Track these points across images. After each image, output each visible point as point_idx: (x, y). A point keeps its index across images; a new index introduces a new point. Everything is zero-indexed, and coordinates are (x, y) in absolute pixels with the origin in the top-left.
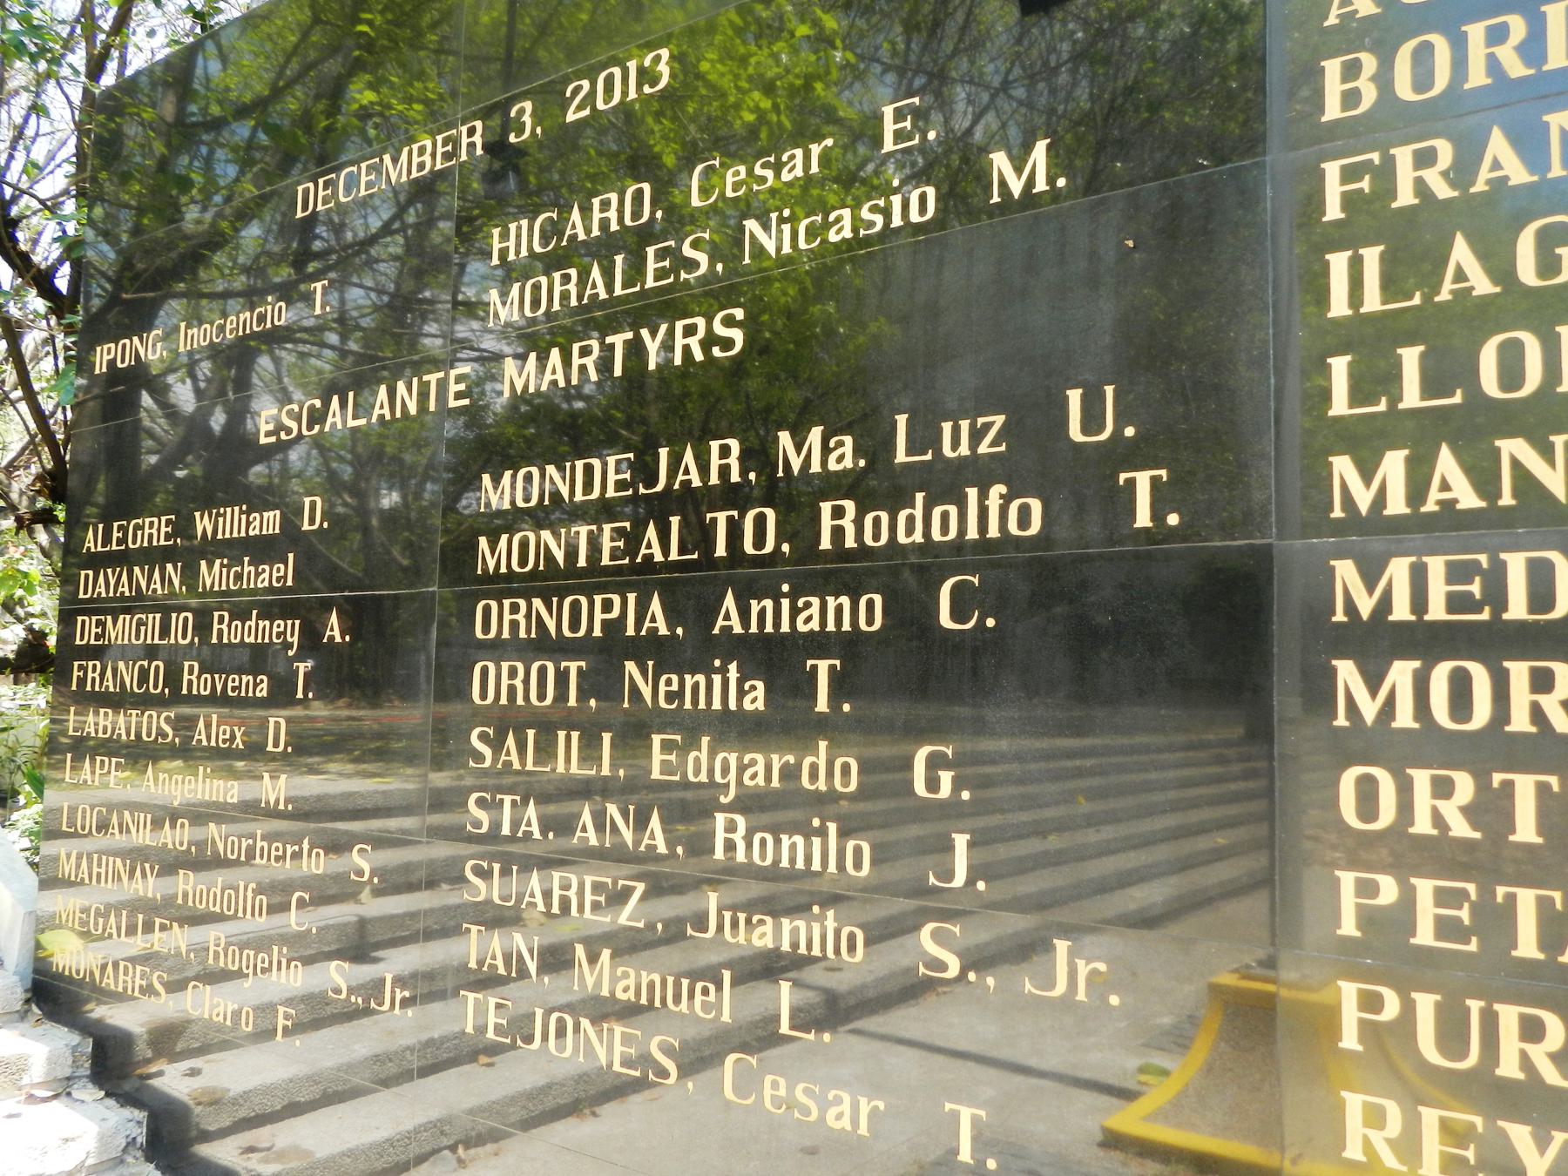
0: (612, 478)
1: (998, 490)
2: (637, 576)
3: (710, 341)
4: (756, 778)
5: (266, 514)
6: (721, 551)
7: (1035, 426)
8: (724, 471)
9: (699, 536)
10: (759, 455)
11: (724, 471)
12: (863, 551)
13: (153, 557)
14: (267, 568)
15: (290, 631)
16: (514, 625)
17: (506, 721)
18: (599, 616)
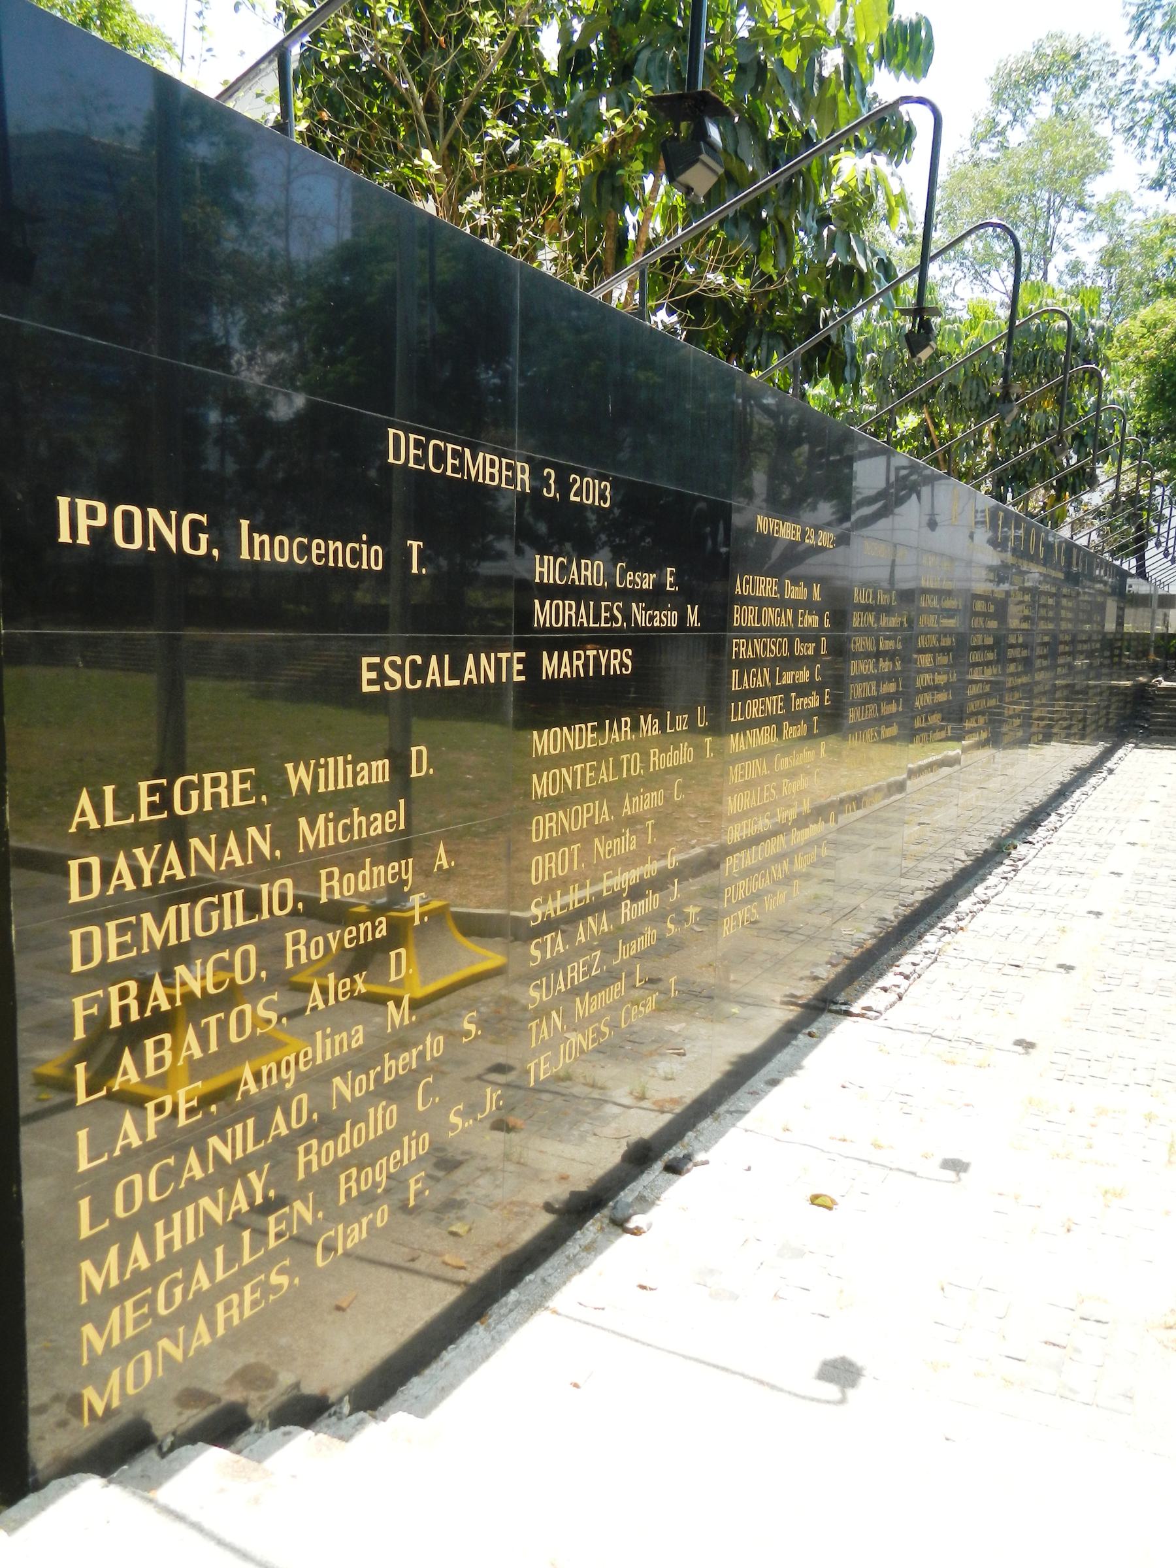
3: (622, 664)
5: (373, 764)
7: (692, 723)
14: (379, 815)
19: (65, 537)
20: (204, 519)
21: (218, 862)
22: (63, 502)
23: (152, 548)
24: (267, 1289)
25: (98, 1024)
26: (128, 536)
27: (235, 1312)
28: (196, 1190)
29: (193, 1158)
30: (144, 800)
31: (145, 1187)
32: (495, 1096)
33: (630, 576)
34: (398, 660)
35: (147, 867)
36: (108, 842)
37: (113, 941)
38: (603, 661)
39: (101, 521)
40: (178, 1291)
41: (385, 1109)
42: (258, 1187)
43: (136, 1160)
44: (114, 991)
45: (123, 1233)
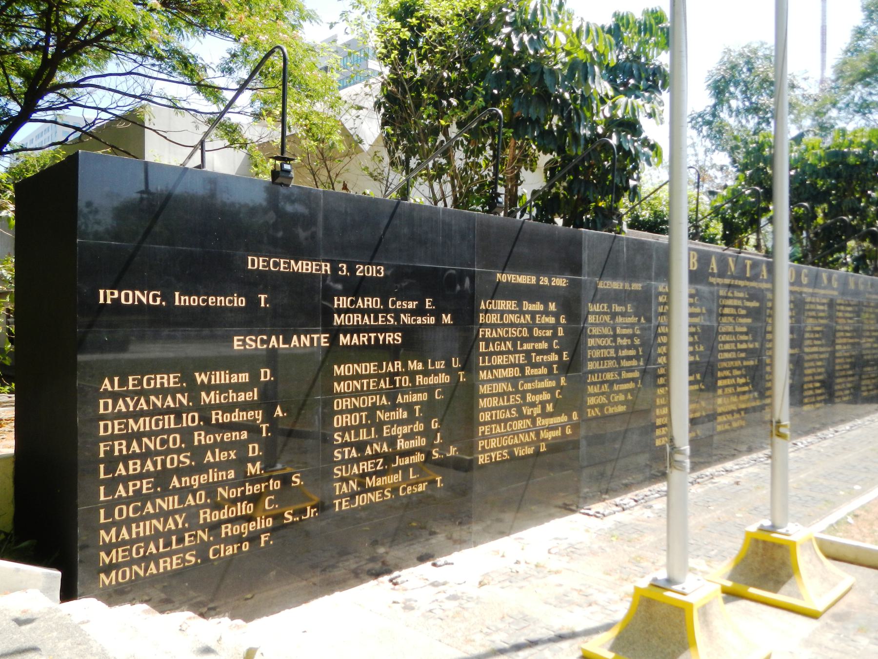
0: (372, 368)
2: (379, 392)
3: (394, 339)
4: (405, 431)
5: (240, 375)
6: (398, 385)
7: (448, 364)
9: (393, 382)
10: (405, 365)
12: (424, 385)
15: (259, 415)
16: (347, 406)
17: (345, 429)
18: (370, 401)
19: (102, 301)
20: (159, 293)
21: (163, 405)
22: (102, 292)
23: (136, 303)
24: (184, 560)
25: (110, 452)
26: (127, 299)
27: (168, 565)
28: (149, 517)
29: (149, 505)
30: (131, 382)
31: (129, 511)
32: (313, 511)
33: (399, 303)
34: (254, 338)
35: (131, 404)
36: (115, 396)
37: (116, 427)
39: (116, 296)
40: (142, 551)
41: (247, 505)
42: (180, 522)
43: (127, 501)
44: (116, 443)
45: (118, 525)
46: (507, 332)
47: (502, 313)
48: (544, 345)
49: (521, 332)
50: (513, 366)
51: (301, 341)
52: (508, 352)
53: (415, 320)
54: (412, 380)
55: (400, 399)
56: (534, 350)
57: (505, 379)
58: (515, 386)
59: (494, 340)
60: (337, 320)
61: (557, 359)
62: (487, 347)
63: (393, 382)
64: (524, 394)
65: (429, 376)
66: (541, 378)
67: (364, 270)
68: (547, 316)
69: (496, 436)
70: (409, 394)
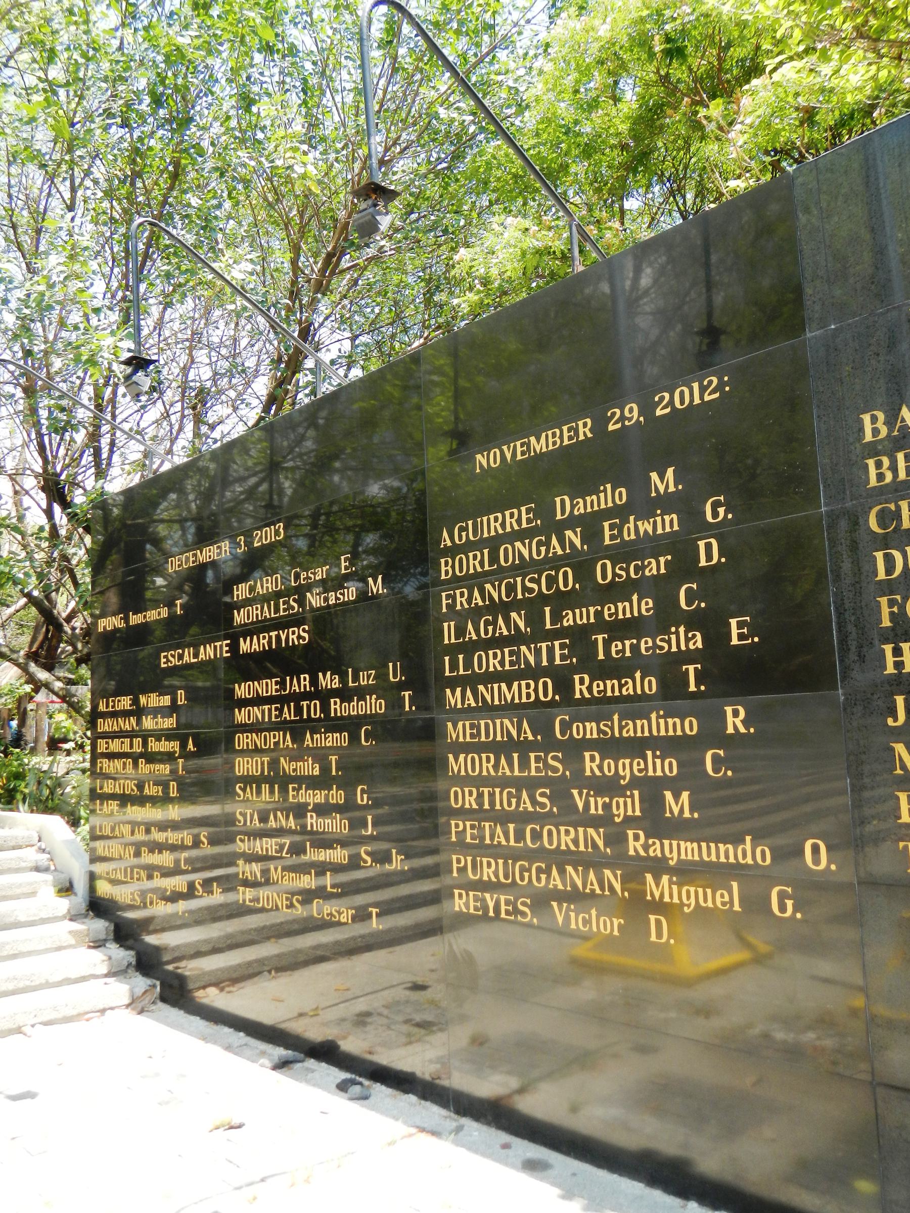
1: (374, 696)
2: (281, 726)
3: (299, 637)
7: (382, 676)
8: (305, 686)
9: (299, 711)
10: (314, 681)
11: (305, 686)
12: (342, 718)
13: (126, 714)
38: (283, 638)
46: (511, 588)
47: (494, 544)
48: (642, 606)
49: (552, 581)
50: (533, 673)
51: (207, 652)
52: (517, 639)
53: (326, 599)
54: (325, 708)
55: (308, 742)
56: (601, 625)
57: (509, 709)
58: (543, 727)
59: (475, 613)
60: (239, 618)
61: (698, 642)
62: (461, 631)
63: (299, 711)
64: (574, 750)
65: (350, 701)
66: (635, 706)
67: (261, 537)
68: (647, 514)
69: (495, 851)
70: (321, 733)
